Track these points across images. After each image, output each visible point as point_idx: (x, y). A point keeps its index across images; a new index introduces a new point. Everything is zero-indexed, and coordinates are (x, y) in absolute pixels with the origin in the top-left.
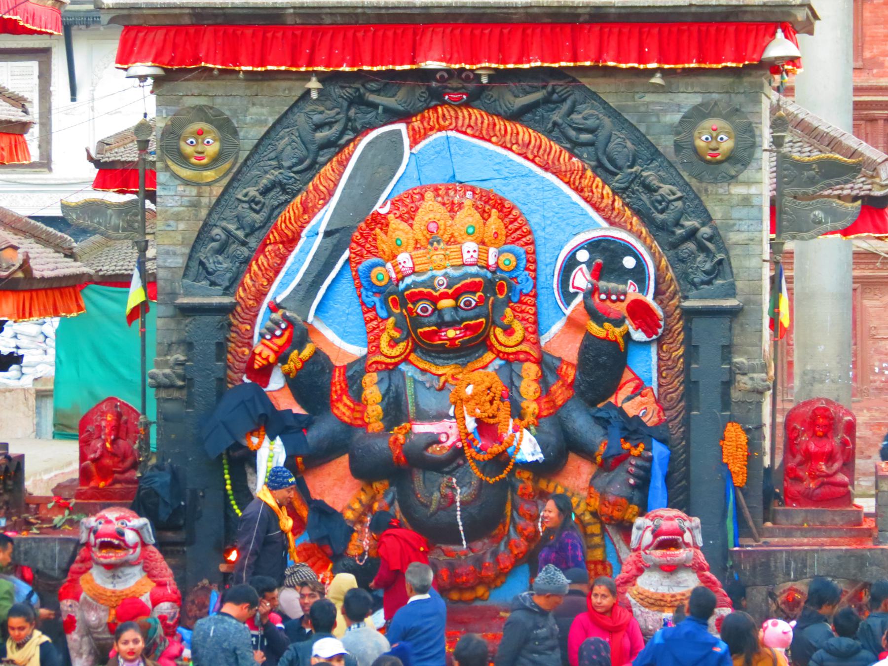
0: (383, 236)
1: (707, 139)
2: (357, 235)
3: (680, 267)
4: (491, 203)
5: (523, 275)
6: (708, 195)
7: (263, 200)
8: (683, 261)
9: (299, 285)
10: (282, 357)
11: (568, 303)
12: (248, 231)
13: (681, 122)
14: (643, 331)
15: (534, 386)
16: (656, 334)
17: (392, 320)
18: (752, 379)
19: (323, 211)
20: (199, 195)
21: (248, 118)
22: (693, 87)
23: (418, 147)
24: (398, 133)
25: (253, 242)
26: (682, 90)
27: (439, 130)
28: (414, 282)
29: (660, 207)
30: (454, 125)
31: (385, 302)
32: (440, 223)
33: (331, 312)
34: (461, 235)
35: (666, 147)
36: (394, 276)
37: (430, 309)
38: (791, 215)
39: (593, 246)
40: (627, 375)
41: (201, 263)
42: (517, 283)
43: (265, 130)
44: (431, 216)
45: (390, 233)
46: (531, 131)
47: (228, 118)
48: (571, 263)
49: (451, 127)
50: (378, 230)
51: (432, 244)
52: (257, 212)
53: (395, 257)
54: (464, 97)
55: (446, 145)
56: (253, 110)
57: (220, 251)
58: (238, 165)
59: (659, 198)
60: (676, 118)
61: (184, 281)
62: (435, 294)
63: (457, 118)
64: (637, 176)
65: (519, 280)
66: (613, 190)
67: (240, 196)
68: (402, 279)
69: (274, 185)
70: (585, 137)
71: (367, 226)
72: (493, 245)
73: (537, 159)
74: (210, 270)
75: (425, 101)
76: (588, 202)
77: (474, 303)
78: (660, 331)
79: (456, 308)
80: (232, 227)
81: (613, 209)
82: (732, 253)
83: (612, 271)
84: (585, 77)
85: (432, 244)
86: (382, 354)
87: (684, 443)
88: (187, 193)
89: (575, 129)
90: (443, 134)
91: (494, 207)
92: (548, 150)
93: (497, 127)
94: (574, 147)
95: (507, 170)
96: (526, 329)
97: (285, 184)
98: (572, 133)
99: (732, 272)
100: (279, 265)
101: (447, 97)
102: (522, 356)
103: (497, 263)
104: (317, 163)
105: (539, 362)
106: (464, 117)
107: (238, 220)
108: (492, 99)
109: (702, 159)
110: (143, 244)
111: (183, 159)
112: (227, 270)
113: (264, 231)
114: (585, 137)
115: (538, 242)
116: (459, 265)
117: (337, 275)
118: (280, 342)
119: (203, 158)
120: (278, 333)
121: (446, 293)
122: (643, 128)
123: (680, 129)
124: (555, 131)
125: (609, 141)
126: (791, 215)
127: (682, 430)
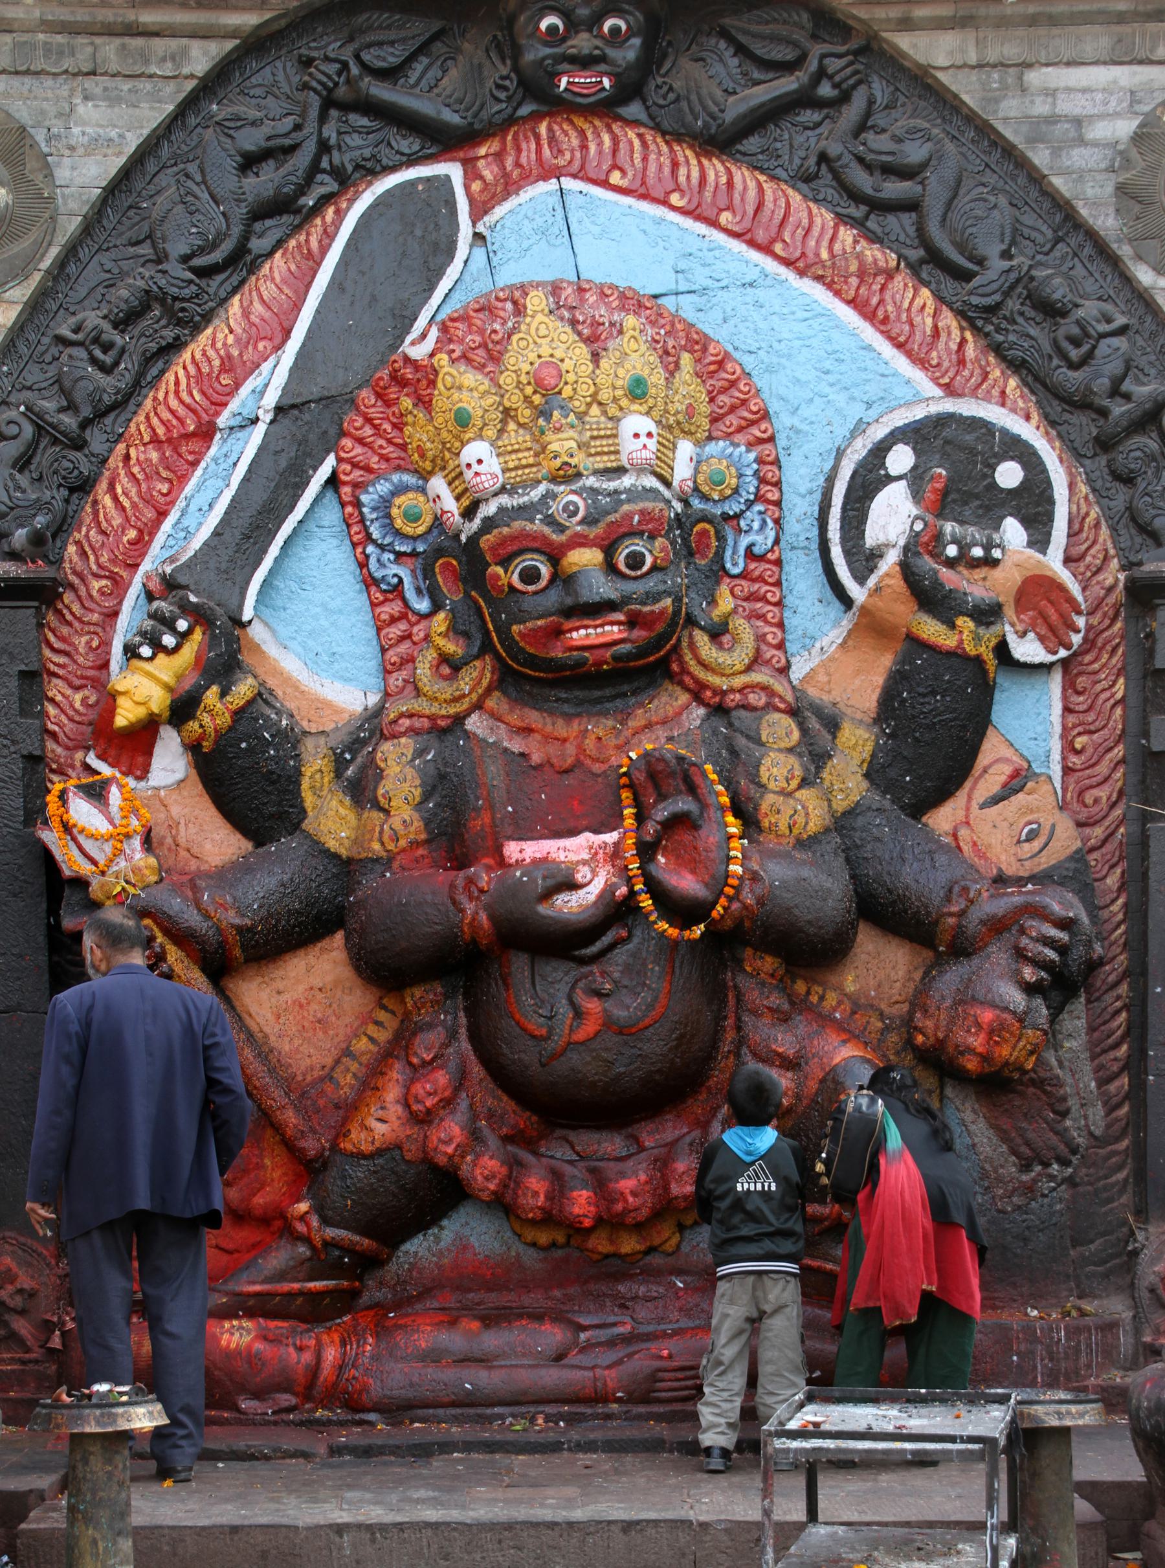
2: (350, 414)
3: (1121, 496)
4: (680, 342)
7: (118, 340)
8: (1127, 479)
12: (86, 411)
13: (1138, 138)
19: (266, 367)
26: (1142, 55)
27: (545, 178)
29: (1074, 354)
32: (564, 367)
34: (615, 400)
40: (991, 749)
42: (739, 531)
43: (121, 161)
46: (762, 178)
54: (606, 83)
55: (560, 210)
59: (1076, 330)
63: (584, 147)
66: (960, 314)
67: (65, 332)
69: (147, 300)
70: (894, 188)
71: (379, 396)
75: (509, 98)
76: (900, 346)
80: (49, 405)
81: (962, 362)
83: (967, 498)
84: (906, 24)
90: (553, 184)
91: (684, 348)
92: (805, 222)
93: (682, 171)
94: (866, 210)
95: (707, 271)
97: (175, 299)
98: (863, 180)
104: (249, 251)
106: (600, 144)
107: (62, 390)
108: (671, 96)
114: (894, 188)
115: (781, 442)
124: (817, 175)
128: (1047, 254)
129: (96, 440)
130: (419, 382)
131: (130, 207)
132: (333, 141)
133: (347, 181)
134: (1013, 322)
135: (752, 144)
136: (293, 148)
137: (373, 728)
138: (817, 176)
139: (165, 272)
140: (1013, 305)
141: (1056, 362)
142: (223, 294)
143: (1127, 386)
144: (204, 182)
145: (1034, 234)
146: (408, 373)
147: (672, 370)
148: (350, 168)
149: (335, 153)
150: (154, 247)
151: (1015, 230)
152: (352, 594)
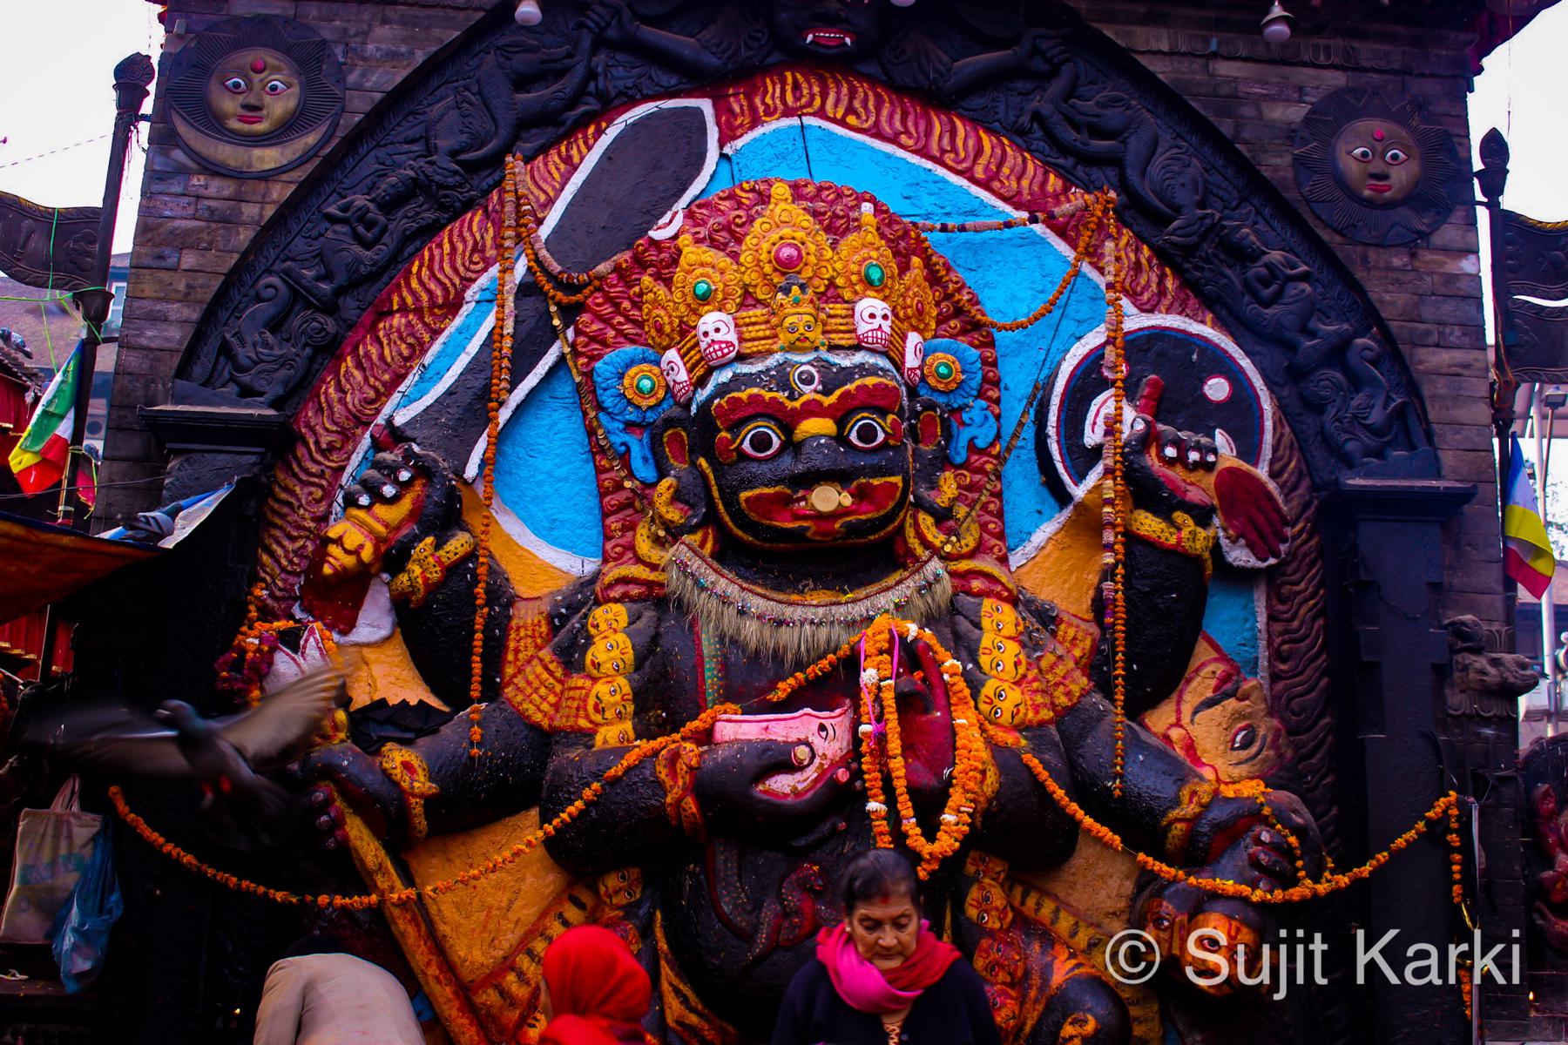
0: (662, 291)
1: (1364, 155)
5: (976, 410)
6: (1369, 270)
9: (450, 393)
10: (393, 556)
11: (1079, 477)
12: (341, 279)
13: (1307, 121)
14: (1251, 546)
15: (1012, 648)
16: (1276, 555)
17: (665, 483)
18: (1495, 663)
20: (238, 199)
21: (371, 47)
22: (1328, 57)
23: (739, 143)
24: (698, 112)
25: (349, 305)
26: (1306, 58)
28: (736, 376)
29: (1266, 292)
30: (818, 102)
31: (655, 447)
33: (524, 473)
35: (1275, 168)
36: (683, 376)
37: (776, 443)
38: (1526, 332)
39: (1139, 347)
40: (1203, 651)
41: (225, 350)
42: (963, 424)
44: (786, 231)
45: (679, 276)
47: (324, 42)
48: (1088, 382)
49: (810, 110)
50: (647, 280)
51: (786, 291)
52: (368, 246)
53: (685, 330)
54: (848, 40)
55: (800, 144)
56: (382, 31)
57: (276, 325)
58: (335, 142)
60: (1296, 113)
61: (179, 381)
62: (790, 405)
64: (1216, 227)
65: (965, 417)
66: (1157, 251)
67: (332, 210)
68: (701, 382)
70: (1100, 144)
72: (915, 329)
73: (996, 185)
74: (244, 361)
77: (881, 436)
78: (1283, 548)
79: (841, 438)
82: (1426, 391)
85: (786, 291)
86: (639, 560)
87: (1334, 811)
88: (212, 191)
89: (1076, 127)
90: (795, 121)
94: (1075, 159)
95: (933, 199)
96: (983, 527)
97: (441, 186)
99: (1429, 436)
100: (406, 359)
101: (810, 37)
102: (976, 584)
103: (921, 368)
105: (1014, 601)
106: (838, 93)
107: (322, 261)
109: (1352, 195)
110: (98, 301)
111: (213, 123)
112: (284, 362)
113: (379, 285)
116: (850, 348)
117: (542, 381)
118: (394, 514)
119: (259, 120)
120: (389, 491)
121: (818, 403)
122: (1226, 127)
123: (1305, 134)
125: (1153, 153)
126: (1526, 332)
127: (1328, 780)
128: (1233, 210)
129: (349, 305)
130: (665, 262)
131: (411, 113)
132: (600, 70)
133: (608, 109)
134: (1207, 260)
135: (978, 102)
136: (560, 74)
137: (586, 595)
138: (1030, 131)
139: (432, 163)
140: (1208, 249)
141: (1247, 298)
142: (484, 186)
143: (1314, 324)
144: (480, 93)
145: (1221, 193)
146: (651, 255)
147: (904, 268)
148: (613, 94)
149: (601, 79)
150: (427, 143)
151: (1205, 187)
152: (578, 464)
